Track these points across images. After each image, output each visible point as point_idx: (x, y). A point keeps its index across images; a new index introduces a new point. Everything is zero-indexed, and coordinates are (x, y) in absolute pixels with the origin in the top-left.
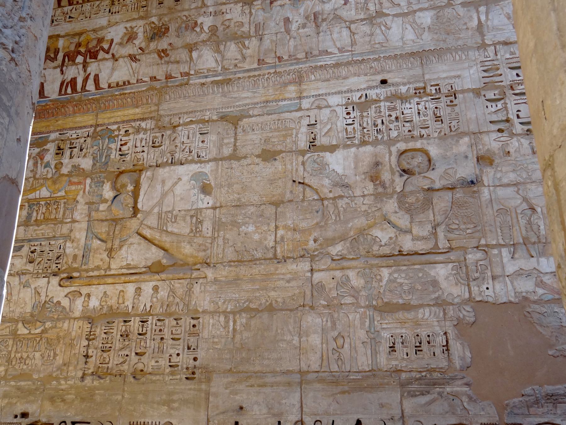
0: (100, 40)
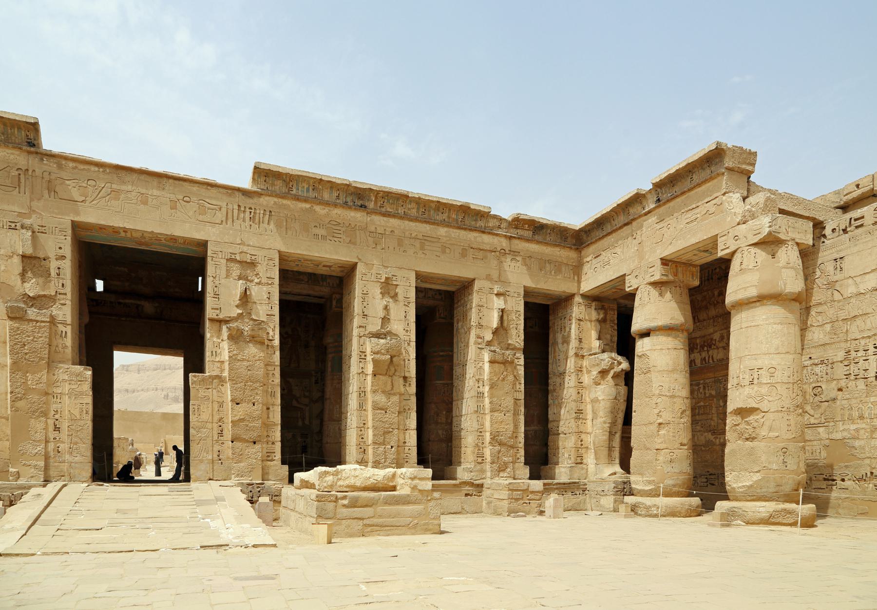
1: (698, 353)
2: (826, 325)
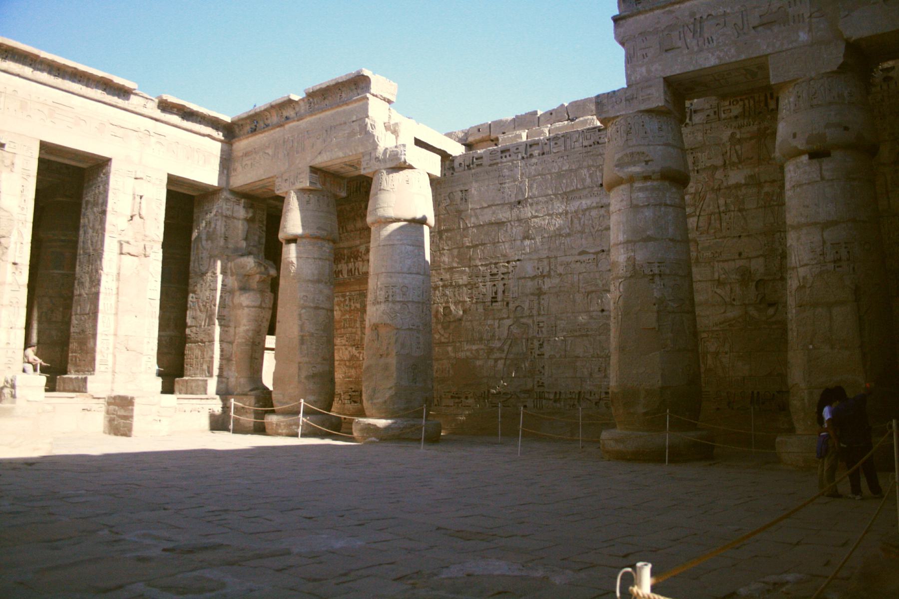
0: (358, 251)
2: (454, 250)
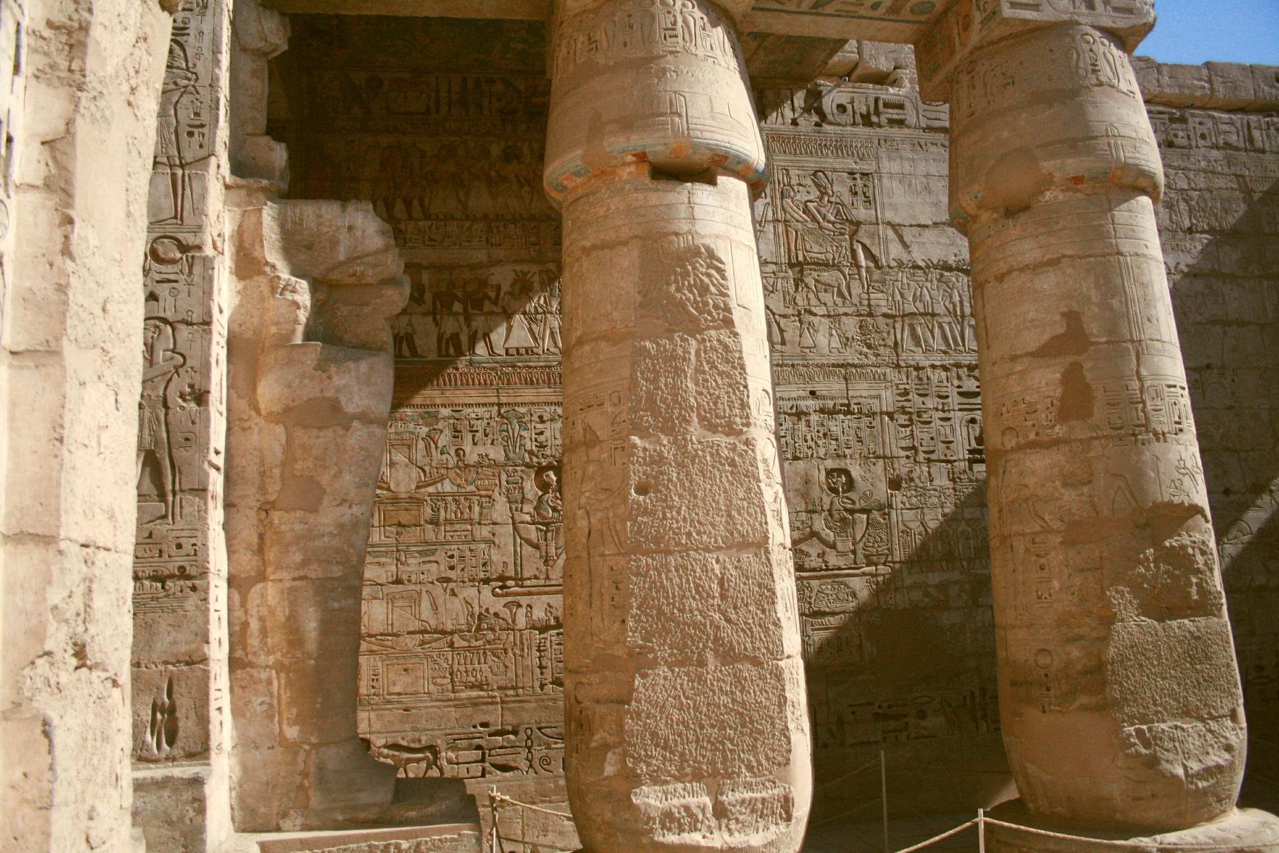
0: (483, 283)
1: (425, 314)
